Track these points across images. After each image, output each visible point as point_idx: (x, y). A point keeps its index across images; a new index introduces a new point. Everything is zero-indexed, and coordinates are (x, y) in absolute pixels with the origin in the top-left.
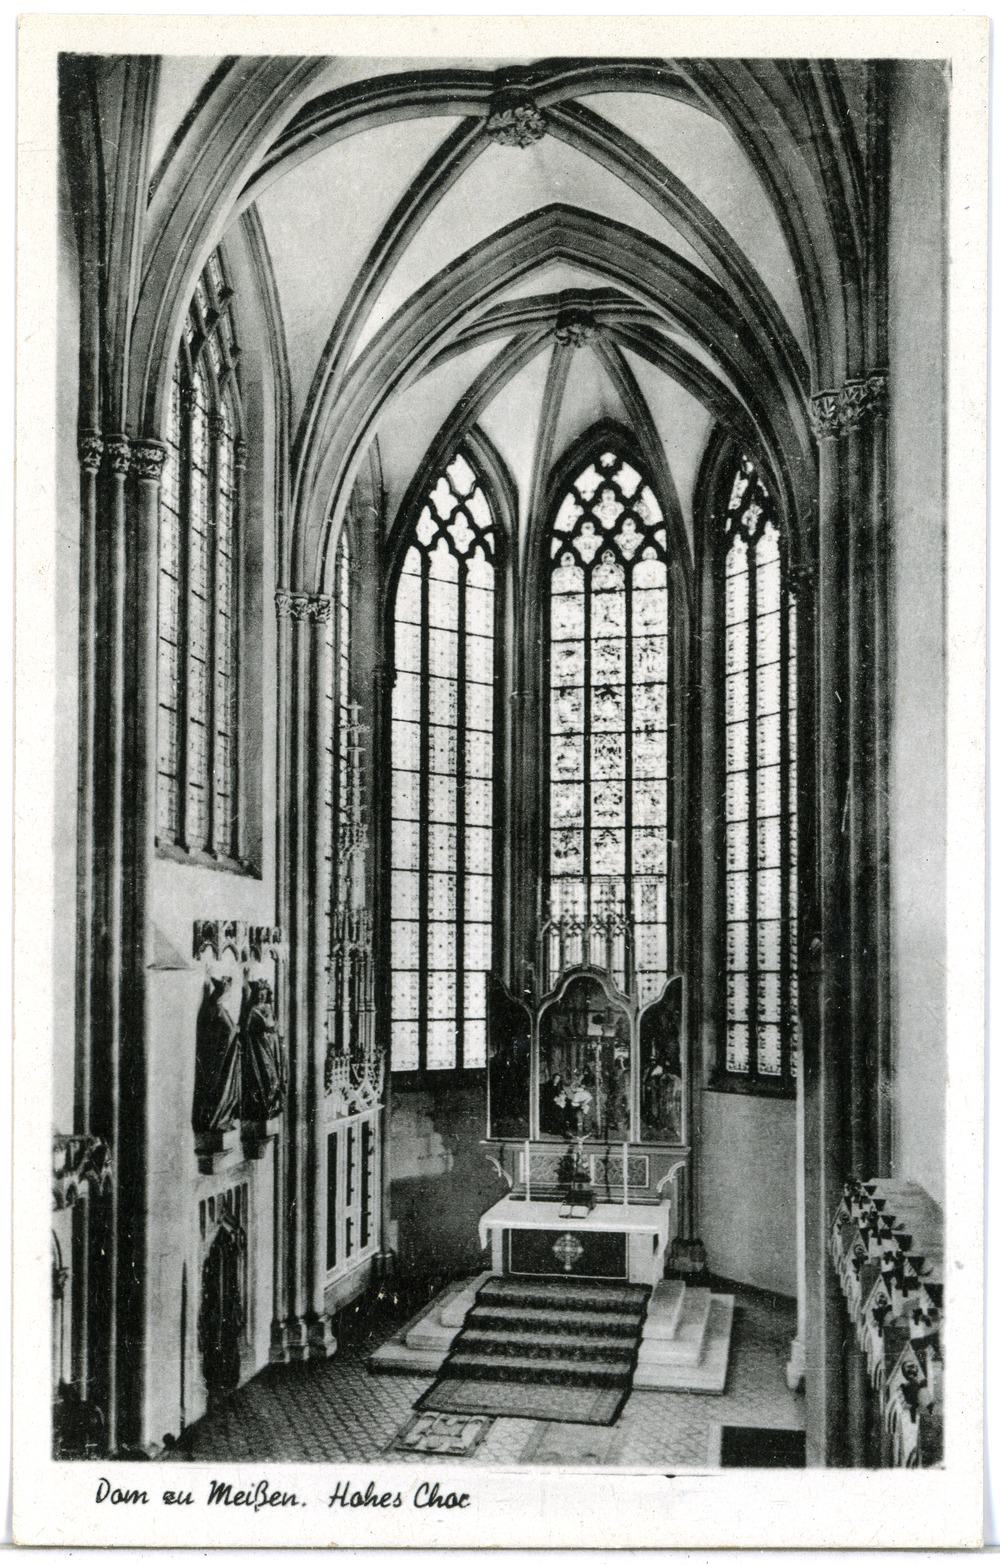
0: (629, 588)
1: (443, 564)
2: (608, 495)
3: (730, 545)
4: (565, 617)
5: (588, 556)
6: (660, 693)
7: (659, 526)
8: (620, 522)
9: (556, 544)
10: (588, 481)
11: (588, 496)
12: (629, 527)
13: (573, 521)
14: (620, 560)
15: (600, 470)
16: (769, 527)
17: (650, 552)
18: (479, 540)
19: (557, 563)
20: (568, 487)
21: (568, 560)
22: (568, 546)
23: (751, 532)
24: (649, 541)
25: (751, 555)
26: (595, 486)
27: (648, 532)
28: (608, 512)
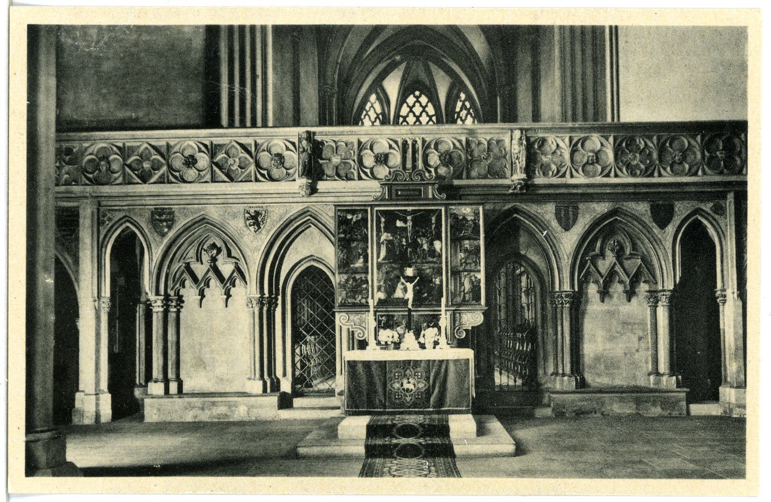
2: (417, 104)
7: (433, 116)
8: (421, 113)
9: (401, 119)
10: (411, 100)
11: (411, 105)
12: (424, 114)
13: (407, 112)
15: (415, 96)
18: (378, 117)
22: (405, 120)
23: (463, 118)
26: (413, 102)
27: (430, 117)
28: (417, 110)
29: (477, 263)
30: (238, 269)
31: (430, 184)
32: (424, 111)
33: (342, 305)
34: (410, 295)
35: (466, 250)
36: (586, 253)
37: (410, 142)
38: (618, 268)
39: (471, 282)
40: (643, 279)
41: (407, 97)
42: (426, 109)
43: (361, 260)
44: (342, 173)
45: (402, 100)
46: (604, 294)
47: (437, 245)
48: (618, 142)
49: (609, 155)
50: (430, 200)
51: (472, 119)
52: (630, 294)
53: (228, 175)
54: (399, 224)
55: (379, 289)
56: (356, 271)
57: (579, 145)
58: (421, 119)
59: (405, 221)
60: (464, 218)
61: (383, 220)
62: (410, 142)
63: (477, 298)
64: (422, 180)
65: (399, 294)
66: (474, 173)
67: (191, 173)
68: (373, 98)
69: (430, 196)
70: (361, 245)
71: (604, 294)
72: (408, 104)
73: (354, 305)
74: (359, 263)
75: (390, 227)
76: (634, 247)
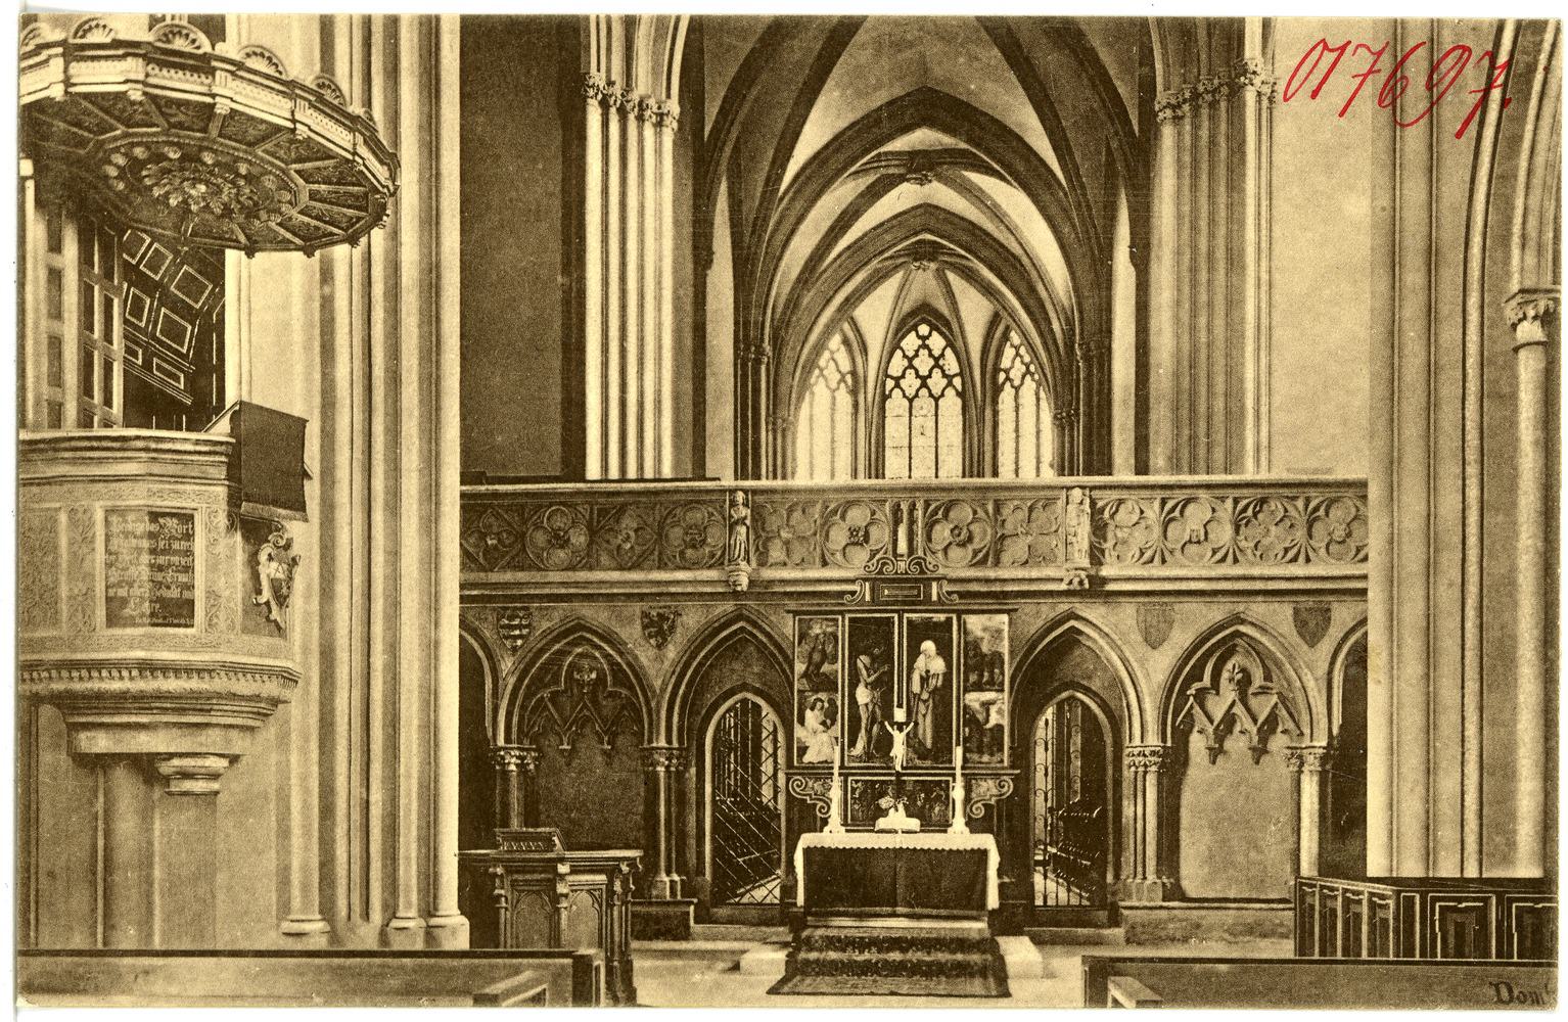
2: (924, 352)
4: (895, 430)
9: (890, 383)
10: (910, 342)
11: (910, 354)
12: (937, 373)
14: (931, 395)
17: (950, 392)
18: (843, 380)
19: (890, 396)
20: (896, 346)
21: (897, 393)
22: (898, 385)
24: (950, 384)
27: (949, 378)
28: (924, 364)
31: (934, 579)
32: (937, 365)
36: (1186, 685)
37: (904, 507)
38: (1239, 710)
40: (1280, 729)
41: (903, 337)
48: (1239, 507)
50: (934, 603)
51: (1034, 385)
52: (1260, 752)
62: (904, 507)
64: (922, 572)
66: (1006, 558)
67: (561, 555)
68: (835, 342)
69: (934, 598)
71: (1216, 753)
76: (1268, 677)
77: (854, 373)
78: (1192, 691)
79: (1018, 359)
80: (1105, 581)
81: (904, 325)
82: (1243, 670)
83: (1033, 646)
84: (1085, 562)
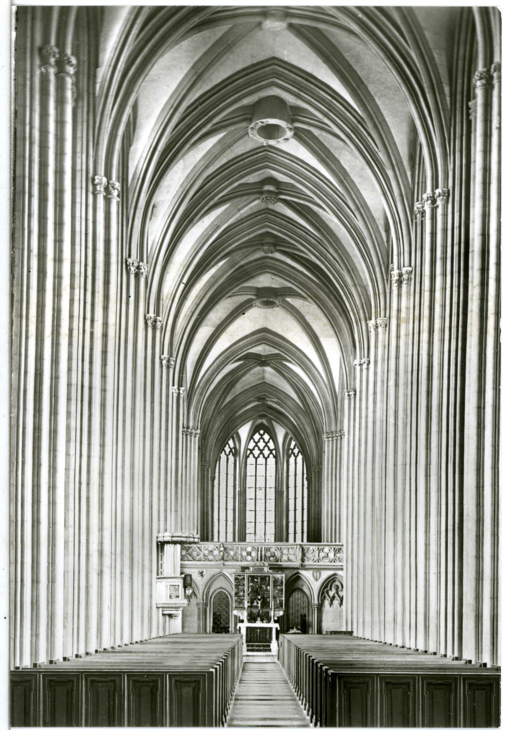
0: (266, 464)
1: (223, 456)
2: (261, 440)
3: (291, 457)
4: (250, 470)
5: (256, 456)
6: (273, 490)
7: (273, 449)
8: (264, 447)
10: (257, 437)
11: (256, 440)
12: (266, 448)
14: (264, 457)
15: (260, 434)
16: (300, 454)
17: (271, 456)
18: (231, 451)
19: (248, 457)
20: (252, 438)
21: (251, 456)
22: (251, 453)
24: (271, 453)
25: (296, 460)
27: (271, 451)
28: (261, 445)
29: (282, 594)
30: (194, 592)
32: (266, 445)
33: (236, 607)
34: (259, 605)
35: (278, 590)
38: (336, 595)
39: (280, 601)
41: (254, 434)
42: (268, 444)
43: (242, 592)
44: (235, 558)
45: (251, 437)
46: (331, 604)
47: (268, 588)
49: (331, 555)
53: (193, 559)
54: (256, 580)
55: (248, 602)
56: (240, 596)
57: (321, 551)
58: (264, 452)
59: (258, 579)
60: (278, 579)
61: (250, 578)
63: (282, 606)
65: (255, 604)
70: (242, 587)
71: (331, 604)
72: (254, 440)
73: (240, 608)
74: (241, 594)
75: (252, 581)
77: (235, 448)
78: (325, 591)
79: (296, 455)
80: (305, 566)
81: (255, 430)
82: (337, 586)
83: (289, 580)
84: (300, 562)
